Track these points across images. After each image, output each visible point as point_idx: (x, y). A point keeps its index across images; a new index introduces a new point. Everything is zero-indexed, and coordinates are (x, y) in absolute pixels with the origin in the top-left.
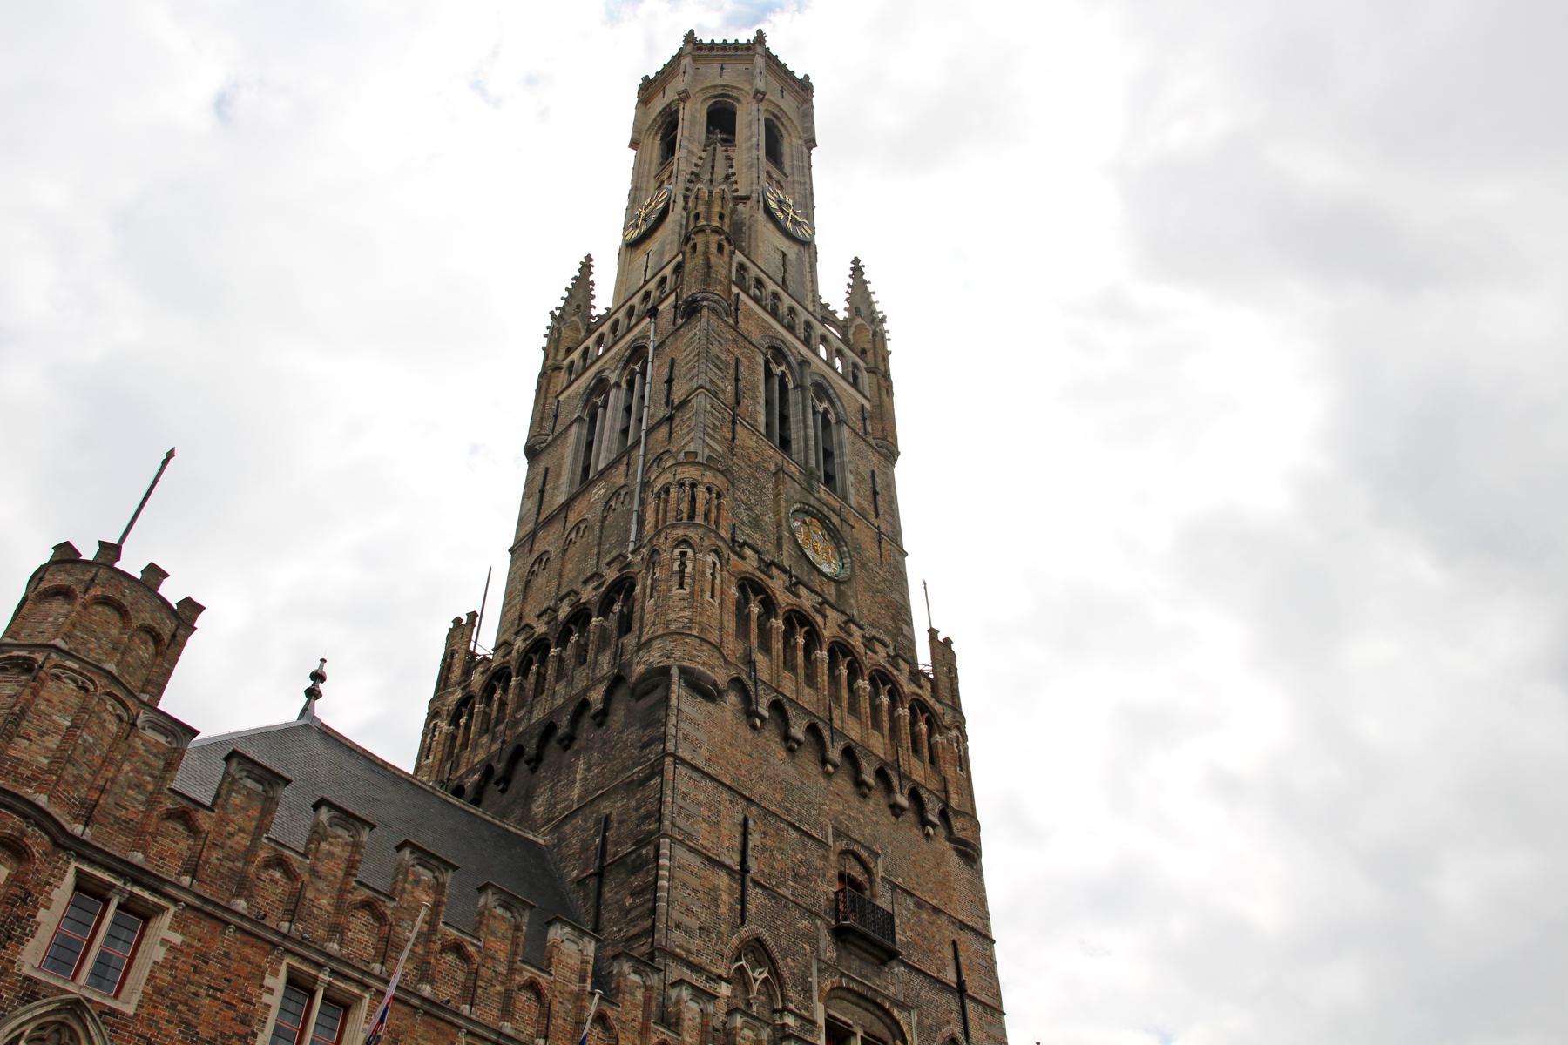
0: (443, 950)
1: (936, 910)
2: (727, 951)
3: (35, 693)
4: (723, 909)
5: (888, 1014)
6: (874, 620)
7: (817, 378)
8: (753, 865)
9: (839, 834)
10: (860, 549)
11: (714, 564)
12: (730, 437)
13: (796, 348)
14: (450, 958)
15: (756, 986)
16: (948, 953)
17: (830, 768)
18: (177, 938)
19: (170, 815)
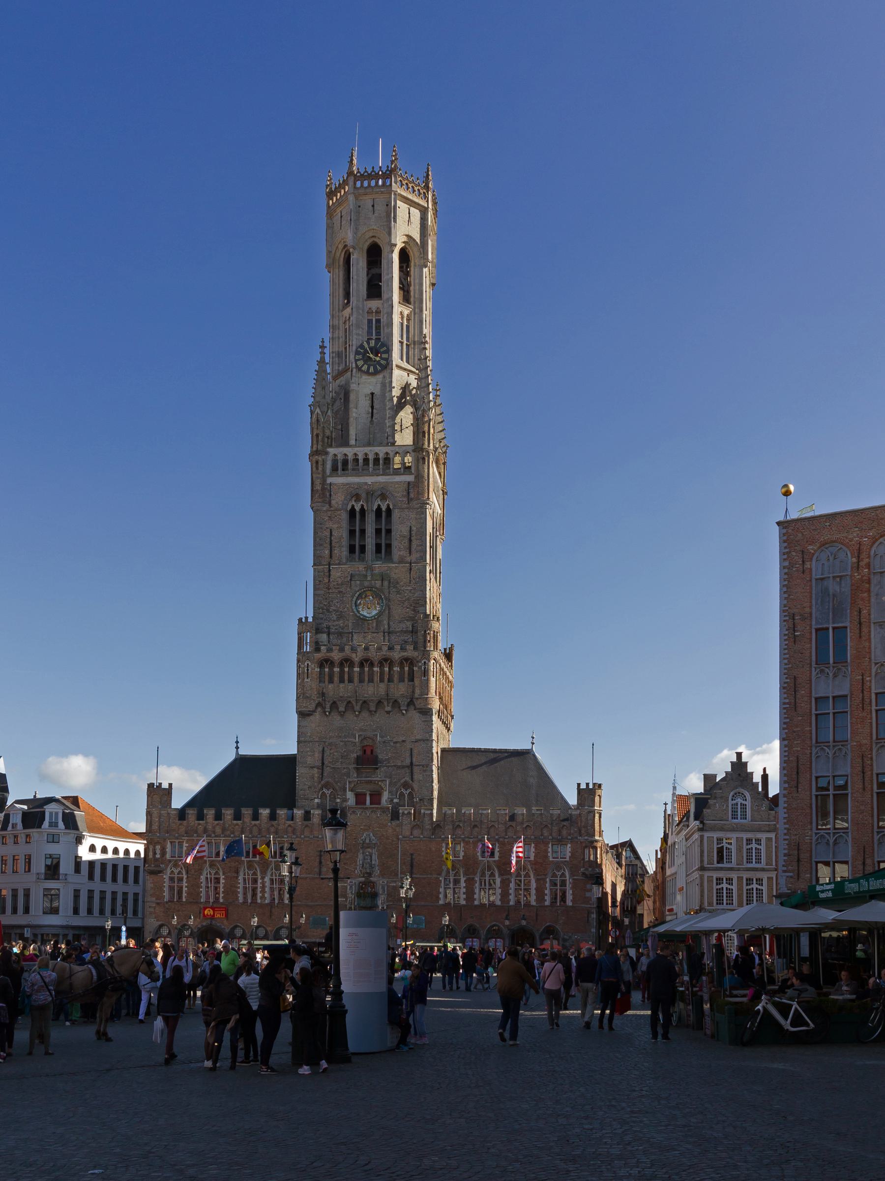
0: (235, 826)
1: (403, 741)
2: (317, 790)
3: (151, 817)
4: (316, 779)
5: (378, 784)
6: (402, 618)
7: (380, 493)
8: (326, 762)
9: (359, 736)
10: (398, 583)
11: (308, 664)
12: (327, 581)
13: (366, 484)
14: (237, 827)
15: (328, 796)
16: (408, 754)
17: (357, 713)
18: (187, 845)
19: (179, 825)
